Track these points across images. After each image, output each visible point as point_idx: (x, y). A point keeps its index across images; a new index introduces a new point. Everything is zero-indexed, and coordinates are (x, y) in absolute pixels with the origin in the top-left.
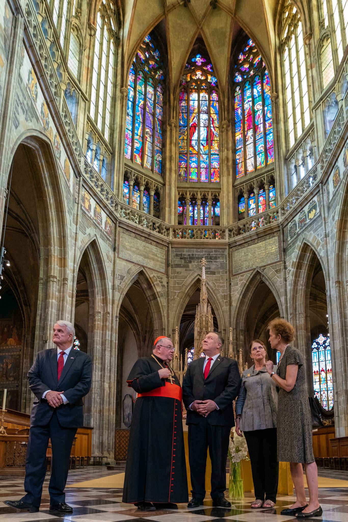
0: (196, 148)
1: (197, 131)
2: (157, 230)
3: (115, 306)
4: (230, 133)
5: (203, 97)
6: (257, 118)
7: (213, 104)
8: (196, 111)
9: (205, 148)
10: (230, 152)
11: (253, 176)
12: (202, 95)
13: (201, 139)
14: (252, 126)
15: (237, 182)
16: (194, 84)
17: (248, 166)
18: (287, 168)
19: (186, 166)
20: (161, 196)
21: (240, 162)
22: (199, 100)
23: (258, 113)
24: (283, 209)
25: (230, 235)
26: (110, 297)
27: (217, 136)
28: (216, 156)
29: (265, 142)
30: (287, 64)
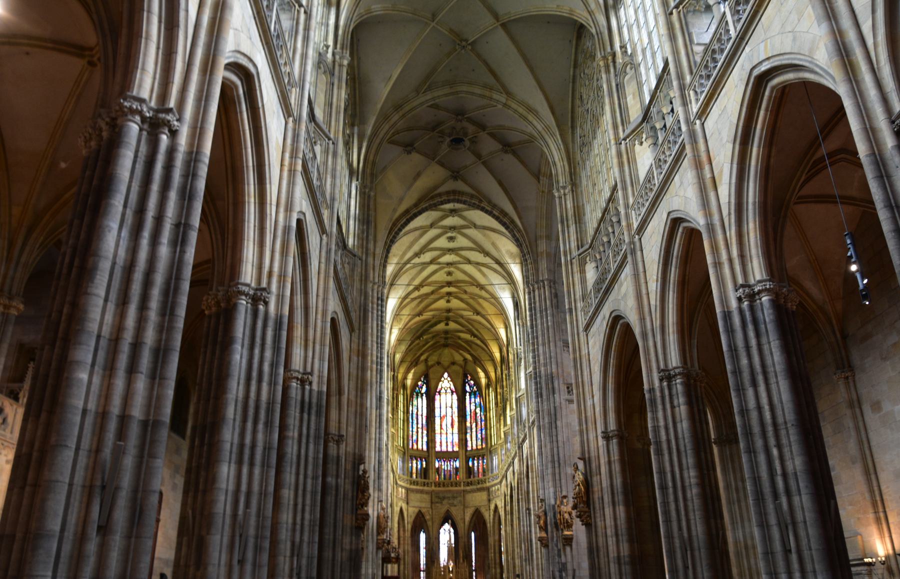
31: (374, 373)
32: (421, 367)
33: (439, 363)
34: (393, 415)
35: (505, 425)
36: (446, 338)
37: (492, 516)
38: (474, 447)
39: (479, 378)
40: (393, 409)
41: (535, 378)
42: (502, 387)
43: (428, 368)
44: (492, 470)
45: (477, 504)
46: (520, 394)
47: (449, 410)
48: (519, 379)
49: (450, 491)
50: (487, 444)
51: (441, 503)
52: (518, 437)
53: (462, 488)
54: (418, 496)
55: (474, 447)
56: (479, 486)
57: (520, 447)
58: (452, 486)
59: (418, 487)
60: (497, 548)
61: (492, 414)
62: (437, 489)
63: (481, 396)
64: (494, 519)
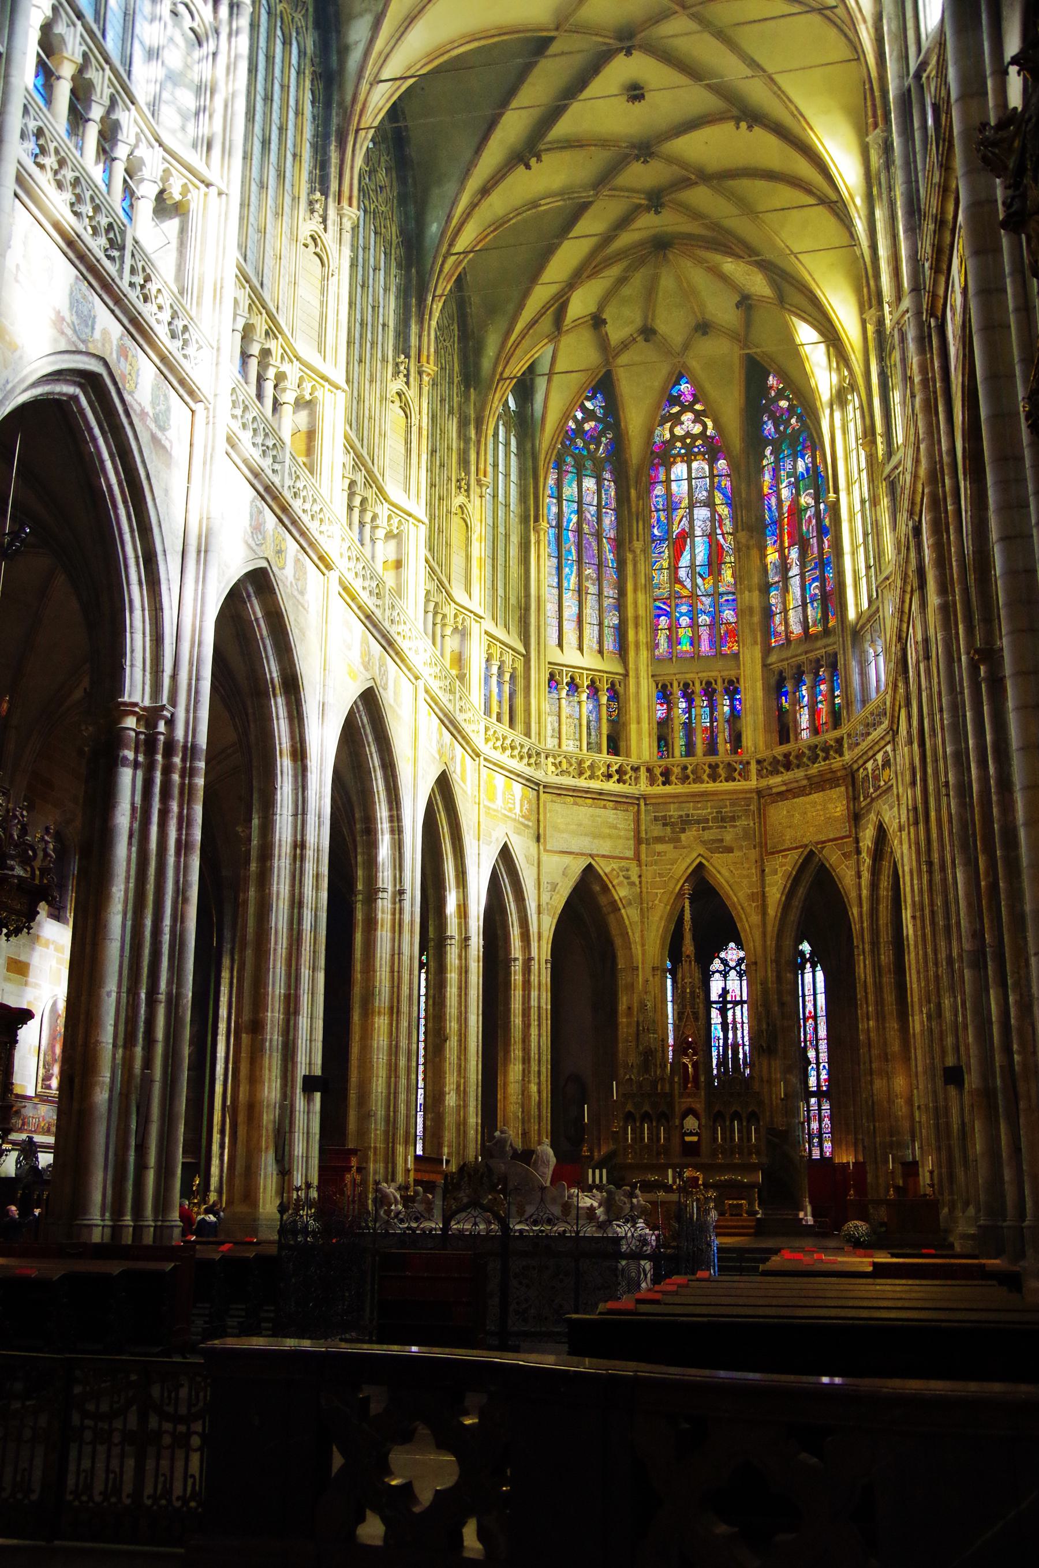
0: (688, 583)
1: (688, 548)
2: (616, 777)
3: (544, 943)
4: (755, 553)
5: (697, 470)
7: (719, 482)
8: (685, 503)
10: (756, 593)
12: (695, 465)
15: (773, 658)
16: (678, 444)
19: (670, 624)
20: (622, 698)
22: (690, 479)
23: (809, 513)
24: (849, 735)
25: (760, 775)
26: (533, 929)
27: (731, 552)
29: (822, 579)
33: (648, 332)
36: (656, 200)
37: (866, 875)
38: (796, 629)
45: (810, 836)
47: (702, 513)
49: (703, 794)
51: (675, 841)
53: (753, 783)
54: (584, 813)
56: (814, 769)
58: (714, 777)
59: (582, 783)
60: (890, 997)
62: (659, 789)
64: (874, 886)
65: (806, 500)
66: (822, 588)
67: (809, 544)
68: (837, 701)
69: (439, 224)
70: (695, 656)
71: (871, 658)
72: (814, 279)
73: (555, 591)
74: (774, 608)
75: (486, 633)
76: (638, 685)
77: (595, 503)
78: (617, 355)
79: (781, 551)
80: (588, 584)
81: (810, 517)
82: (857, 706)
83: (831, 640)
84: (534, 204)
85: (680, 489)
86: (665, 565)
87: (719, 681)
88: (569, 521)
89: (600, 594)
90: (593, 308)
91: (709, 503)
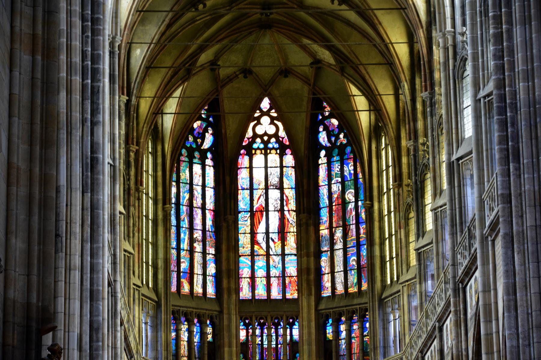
0: (264, 245)
4: (312, 229)
6: (349, 214)
8: (263, 185)
9: (276, 244)
10: (312, 259)
11: (341, 305)
12: (269, 156)
13: (271, 230)
14: (341, 223)
15: (322, 306)
16: (258, 140)
17: (336, 282)
18: (383, 311)
21: (327, 272)
22: (266, 167)
27: (294, 224)
28: (293, 256)
30: (383, 153)
31: (77, 97)
32: (200, 83)
33: (247, 72)
34: (127, 207)
35: (421, 232)
38: (340, 288)
39: (354, 111)
40: (127, 192)
41: (502, 111)
42: (414, 135)
43: (219, 84)
44: (386, 347)
46: (461, 152)
47: (274, 194)
48: (458, 112)
50: (372, 281)
52: (454, 264)
55: (340, 288)
57: (460, 288)
61: (387, 203)
63: (357, 158)
65: (350, 196)
66: (358, 261)
67: (349, 229)
68: (366, 339)
69: (142, 51)
70: (269, 299)
71: (392, 317)
72: (367, 73)
73: (174, 252)
74: (323, 269)
75: (143, 295)
76: (230, 320)
77: (200, 183)
78: (223, 86)
79: (330, 227)
80: (195, 245)
81: (351, 209)
82: (380, 351)
83: (364, 300)
84: (193, 20)
85: (259, 175)
86: (248, 230)
87: (284, 318)
88: (184, 198)
89: (204, 253)
90: (211, 58)
91: (281, 187)
